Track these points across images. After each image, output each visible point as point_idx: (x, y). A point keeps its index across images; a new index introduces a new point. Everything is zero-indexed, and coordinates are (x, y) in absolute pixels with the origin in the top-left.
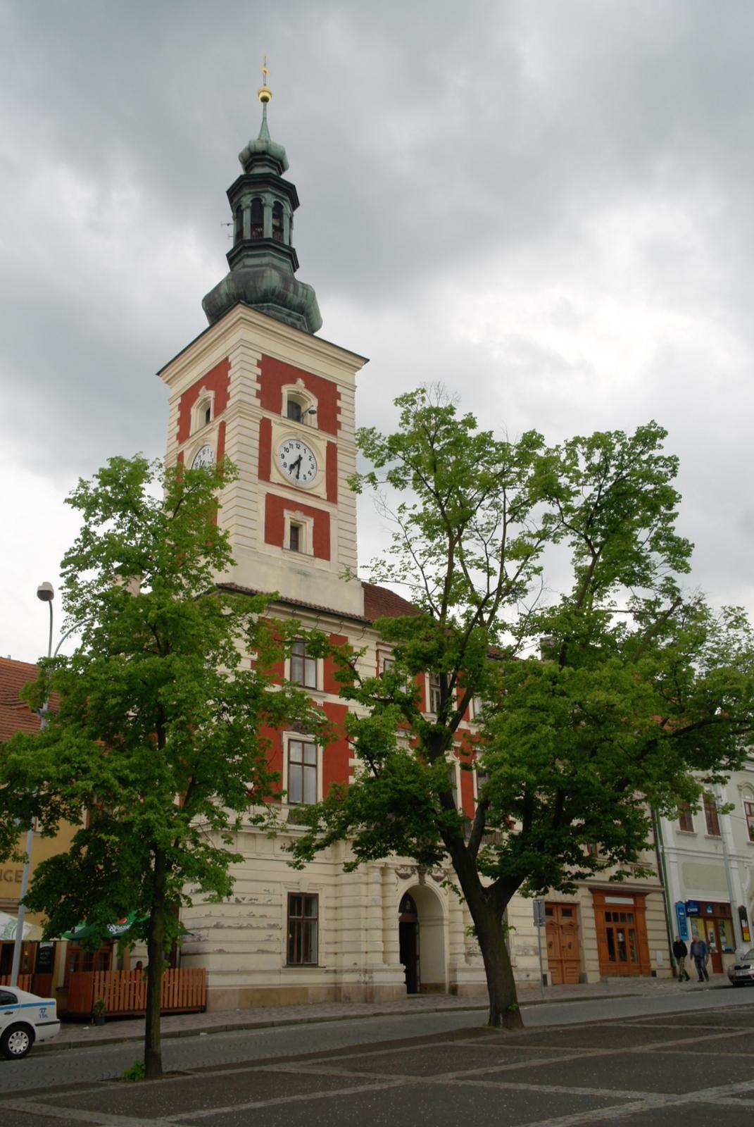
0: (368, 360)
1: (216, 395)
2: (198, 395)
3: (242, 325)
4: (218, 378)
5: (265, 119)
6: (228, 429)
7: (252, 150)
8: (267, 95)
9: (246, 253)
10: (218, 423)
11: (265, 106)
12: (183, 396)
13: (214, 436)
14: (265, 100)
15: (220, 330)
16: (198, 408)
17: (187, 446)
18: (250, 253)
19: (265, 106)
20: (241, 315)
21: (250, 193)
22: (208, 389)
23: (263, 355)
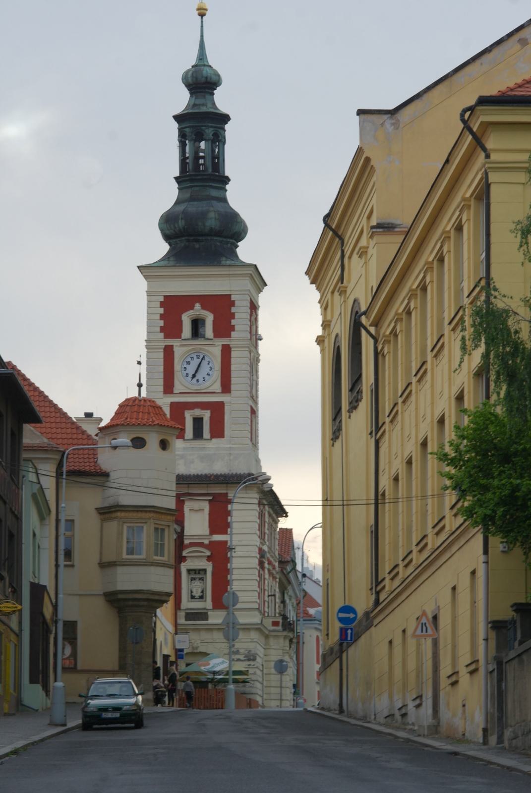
0: (266, 285)
1: (214, 318)
2: (192, 308)
3: (248, 278)
4: (221, 306)
5: (202, 36)
6: (233, 354)
7: (209, 80)
8: (202, 11)
9: (210, 184)
10: (221, 343)
11: (202, 22)
12: (166, 297)
13: (217, 351)
14: (202, 15)
15: (230, 271)
16: (188, 317)
17: (179, 344)
18: (213, 185)
19: (202, 22)
20: (251, 272)
21: (212, 127)
22: (204, 307)
23: (251, 299)
